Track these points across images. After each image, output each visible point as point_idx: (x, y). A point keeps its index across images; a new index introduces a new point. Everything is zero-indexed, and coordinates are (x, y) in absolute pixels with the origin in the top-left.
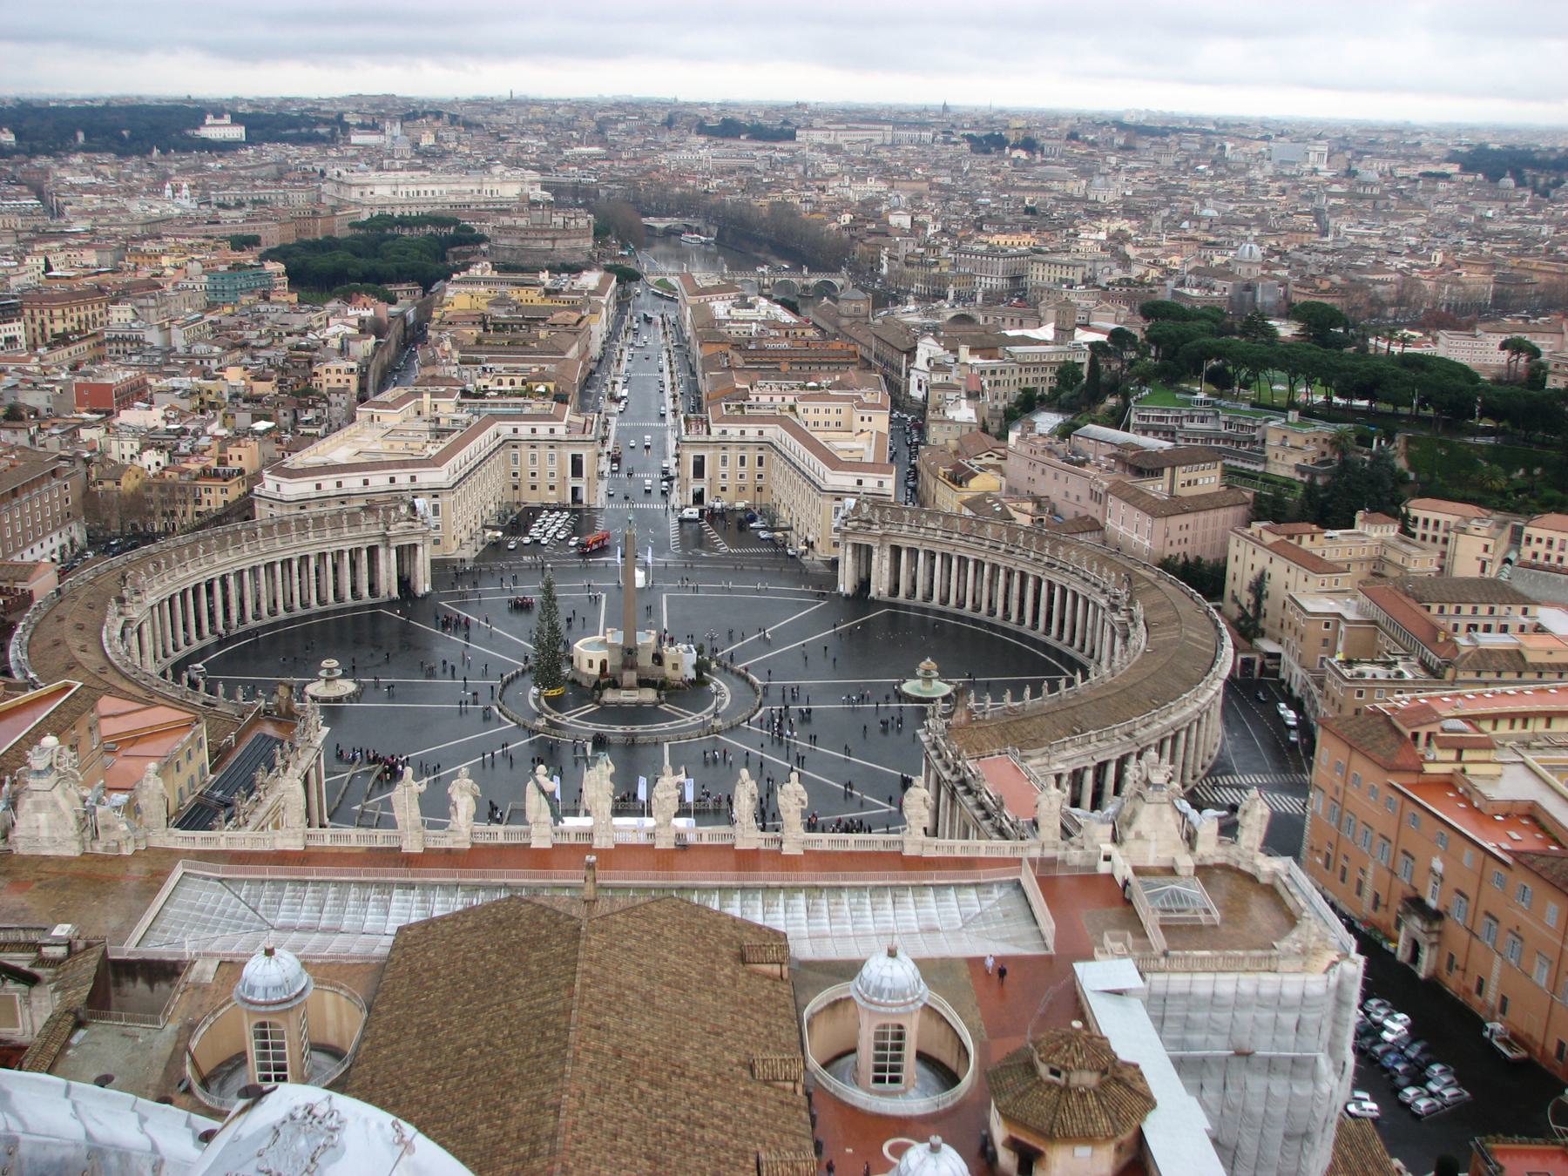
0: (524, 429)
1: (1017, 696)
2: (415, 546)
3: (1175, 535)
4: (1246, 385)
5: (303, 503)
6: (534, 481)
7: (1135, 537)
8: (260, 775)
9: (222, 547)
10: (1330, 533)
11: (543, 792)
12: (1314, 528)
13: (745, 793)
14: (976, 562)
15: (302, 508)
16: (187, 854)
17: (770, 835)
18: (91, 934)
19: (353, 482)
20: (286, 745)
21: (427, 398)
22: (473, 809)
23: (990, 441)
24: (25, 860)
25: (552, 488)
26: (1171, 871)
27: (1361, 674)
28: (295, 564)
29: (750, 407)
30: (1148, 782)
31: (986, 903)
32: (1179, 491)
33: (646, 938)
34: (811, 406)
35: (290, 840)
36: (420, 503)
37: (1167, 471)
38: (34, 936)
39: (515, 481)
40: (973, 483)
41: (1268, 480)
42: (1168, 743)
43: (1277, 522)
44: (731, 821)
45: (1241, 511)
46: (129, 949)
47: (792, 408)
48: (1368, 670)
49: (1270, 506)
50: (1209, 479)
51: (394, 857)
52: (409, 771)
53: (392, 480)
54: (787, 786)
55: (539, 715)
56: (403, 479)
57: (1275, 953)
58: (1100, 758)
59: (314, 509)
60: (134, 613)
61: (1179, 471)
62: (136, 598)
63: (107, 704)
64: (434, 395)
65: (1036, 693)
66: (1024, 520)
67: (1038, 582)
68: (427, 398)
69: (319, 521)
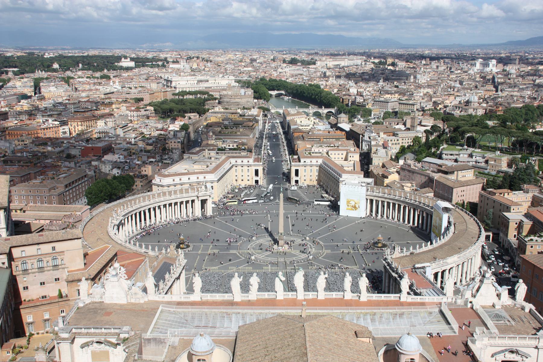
0: (239, 161)
1: (414, 248)
2: (207, 200)
3: (460, 194)
5: (169, 186)
6: (242, 178)
7: (446, 194)
8: (167, 276)
9: (144, 201)
10: (514, 192)
11: (281, 281)
12: (509, 191)
13: (348, 281)
14: (393, 203)
15: (169, 187)
16: (162, 302)
17: (356, 295)
19: (185, 179)
20: (174, 266)
21: (207, 150)
22: (257, 287)
23: (394, 163)
24: (108, 304)
25: (248, 180)
26: (494, 306)
27: (532, 240)
28: (168, 206)
29: (313, 153)
30: (484, 276)
31: (430, 318)
32: (459, 179)
33: (326, 329)
34: (333, 152)
35: (197, 296)
36: (209, 185)
37: (456, 172)
38: (117, 331)
39: (236, 178)
40: (389, 177)
41: (488, 174)
42: (465, 264)
43: (495, 189)
44: (344, 291)
45: (481, 185)
46: (148, 335)
47: (327, 153)
48: (536, 238)
50: (469, 175)
51: (232, 304)
52: (236, 274)
53: (198, 178)
54: (362, 278)
55: (252, 255)
56: (201, 177)
57: (537, 336)
58: (443, 269)
59: (172, 188)
62: (118, 217)
64: (209, 150)
65: (421, 247)
68: (207, 150)
69: (175, 192)
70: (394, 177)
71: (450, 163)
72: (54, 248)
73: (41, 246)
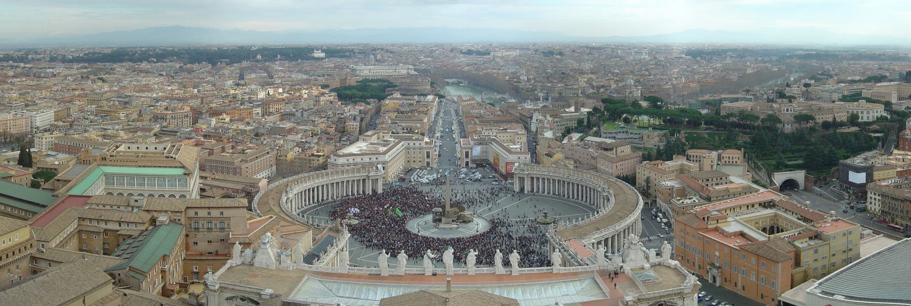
1: (577, 220)
4: (635, 121)
18: (278, 293)
24: (257, 268)
26: (643, 268)
49: (647, 157)
50: (627, 150)
60: (290, 196)
61: (619, 149)
63: (283, 223)
66: (572, 167)
67: (578, 185)
70: (558, 156)
71: (609, 141)
72: (222, 213)
73: (211, 210)
